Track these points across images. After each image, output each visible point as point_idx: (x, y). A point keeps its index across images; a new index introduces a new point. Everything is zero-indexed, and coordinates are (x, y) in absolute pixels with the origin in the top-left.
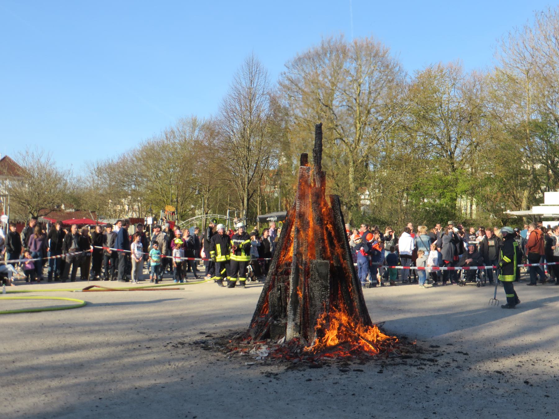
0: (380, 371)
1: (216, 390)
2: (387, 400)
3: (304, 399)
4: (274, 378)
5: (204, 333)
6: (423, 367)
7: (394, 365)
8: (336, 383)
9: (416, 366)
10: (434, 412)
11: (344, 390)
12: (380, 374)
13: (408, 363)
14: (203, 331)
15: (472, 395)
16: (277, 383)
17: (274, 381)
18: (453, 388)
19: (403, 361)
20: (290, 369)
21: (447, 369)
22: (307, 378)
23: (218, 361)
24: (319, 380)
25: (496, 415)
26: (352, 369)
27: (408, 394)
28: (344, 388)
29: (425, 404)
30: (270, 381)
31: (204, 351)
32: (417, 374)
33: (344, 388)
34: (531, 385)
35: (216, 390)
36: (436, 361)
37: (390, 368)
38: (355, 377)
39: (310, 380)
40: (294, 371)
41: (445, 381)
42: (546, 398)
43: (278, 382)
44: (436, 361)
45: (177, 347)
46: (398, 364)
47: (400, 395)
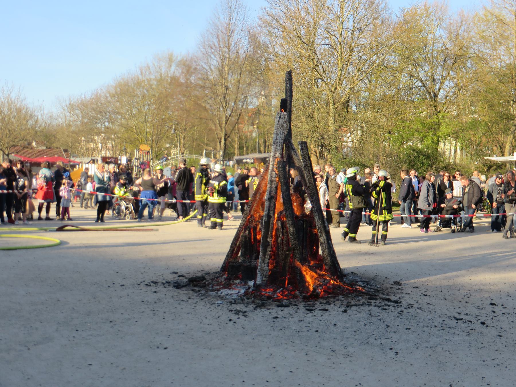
0: (345, 310)
1: (187, 325)
2: (348, 336)
3: (270, 334)
4: (243, 315)
5: (177, 273)
6: (387, 307)
7: (359, 305)
8: (302, 321)
9: (381, 306)
10: (391, 347)
11: (308, 327)
12: (345, 314)
13: (372, 304)
14: (176, 271)
15: (430, 334)
16: (245, 320)
17: (242, 318)
18: (412, 328)
19: (368, 302)
20: (258, 308)
21: (409, 310)
22: (274, 316)
23: (189, 299)
24: (285, 317)
25: (449, 351)
26: (318, 309)
27: (369, 331)
28: (308, 325)
29: (384, 341)
30: (239, 318)
31: (176, 289)
32: (380, 314)
33: (308, 325)
34: (487, 326)
35: (187, 325)
36: (400, 303)
37: (354, 308)
38: (320, 315)
39: (277, 318)
40: (262, 309)
41: (406, 321)
42: (499, 337)
43: (246, 319)
44: (400, 303)
45: (150, 285)
46: (363, 304)
47: (361, 332)
